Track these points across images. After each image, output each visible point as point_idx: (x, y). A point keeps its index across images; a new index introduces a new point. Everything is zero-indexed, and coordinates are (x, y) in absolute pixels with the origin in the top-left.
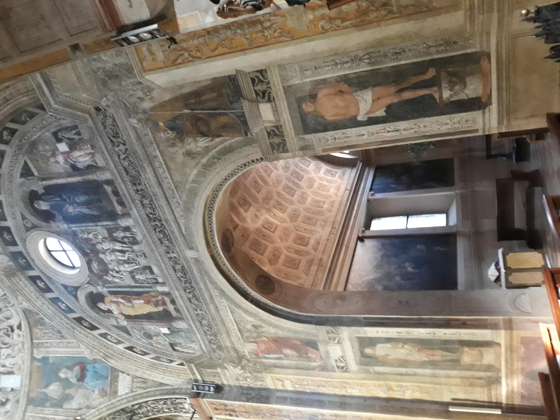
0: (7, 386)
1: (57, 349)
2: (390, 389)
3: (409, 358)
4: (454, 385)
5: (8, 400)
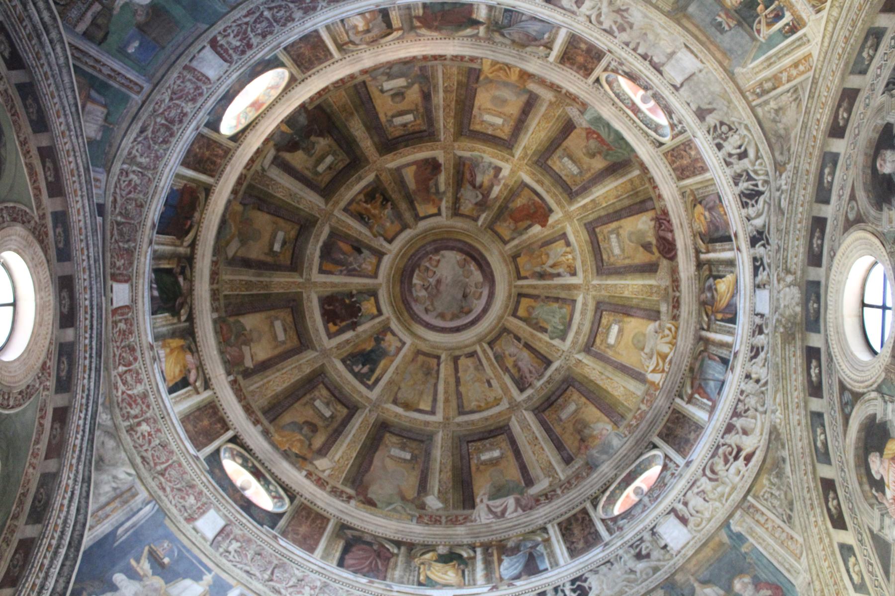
0: (665, 536)
1: (766, 536)
5: (648, 556)
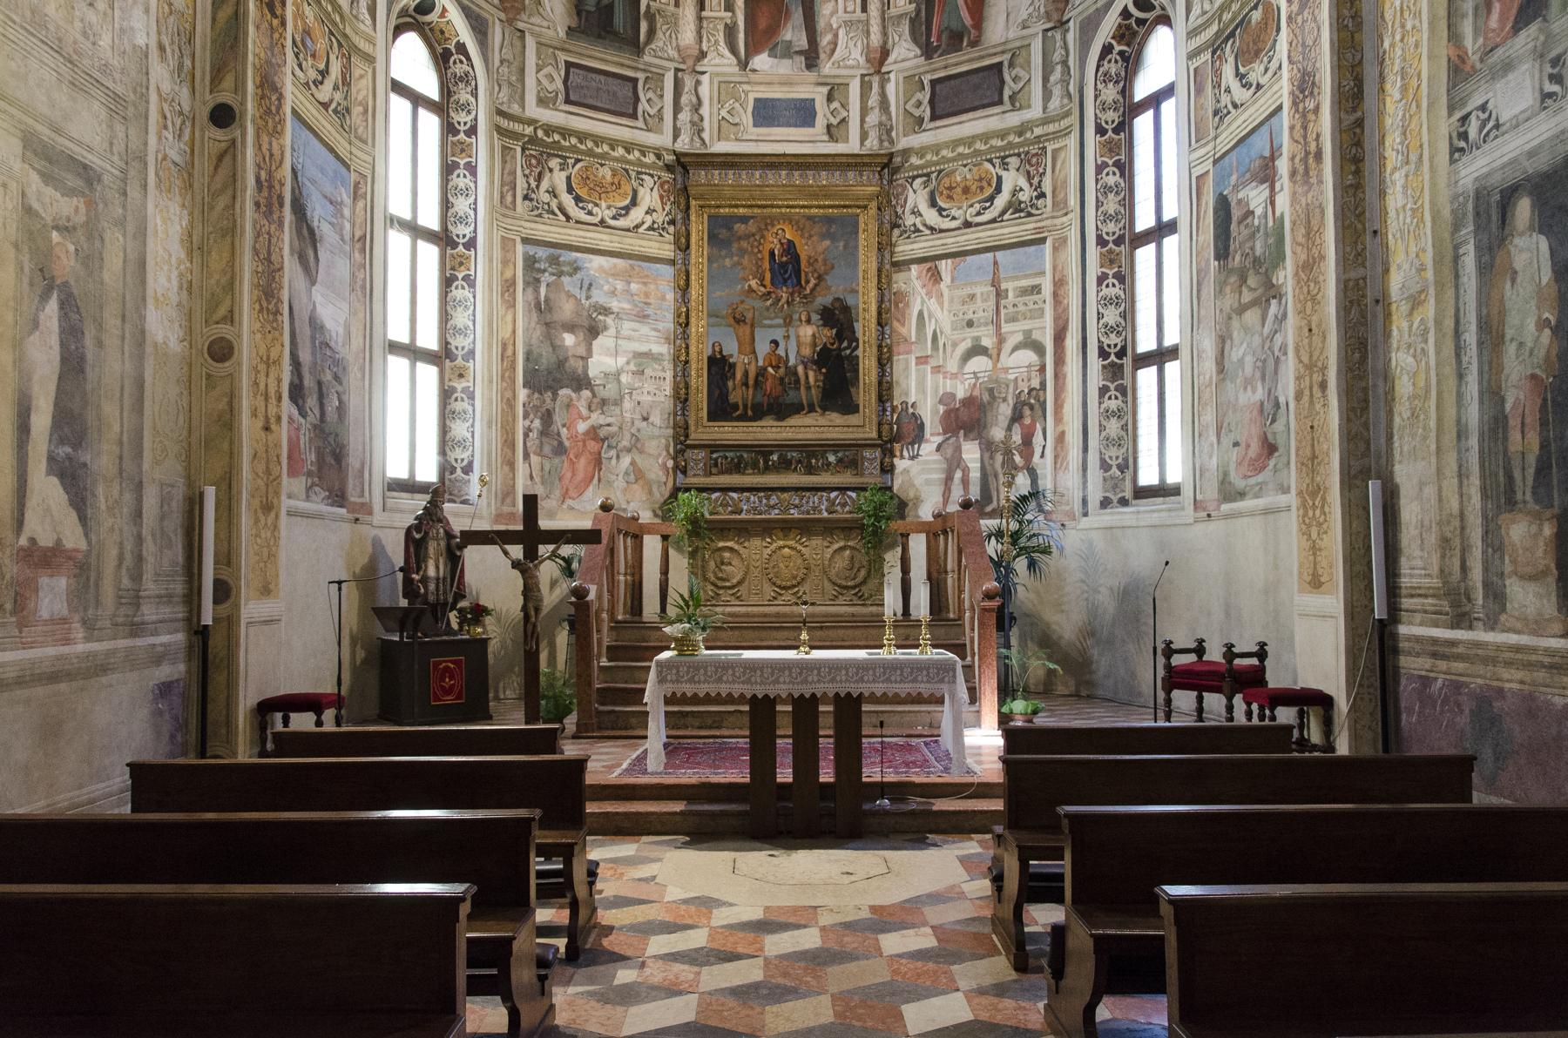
2: (1416, 302)
3: (1511, 349)
4: (1440, 490)
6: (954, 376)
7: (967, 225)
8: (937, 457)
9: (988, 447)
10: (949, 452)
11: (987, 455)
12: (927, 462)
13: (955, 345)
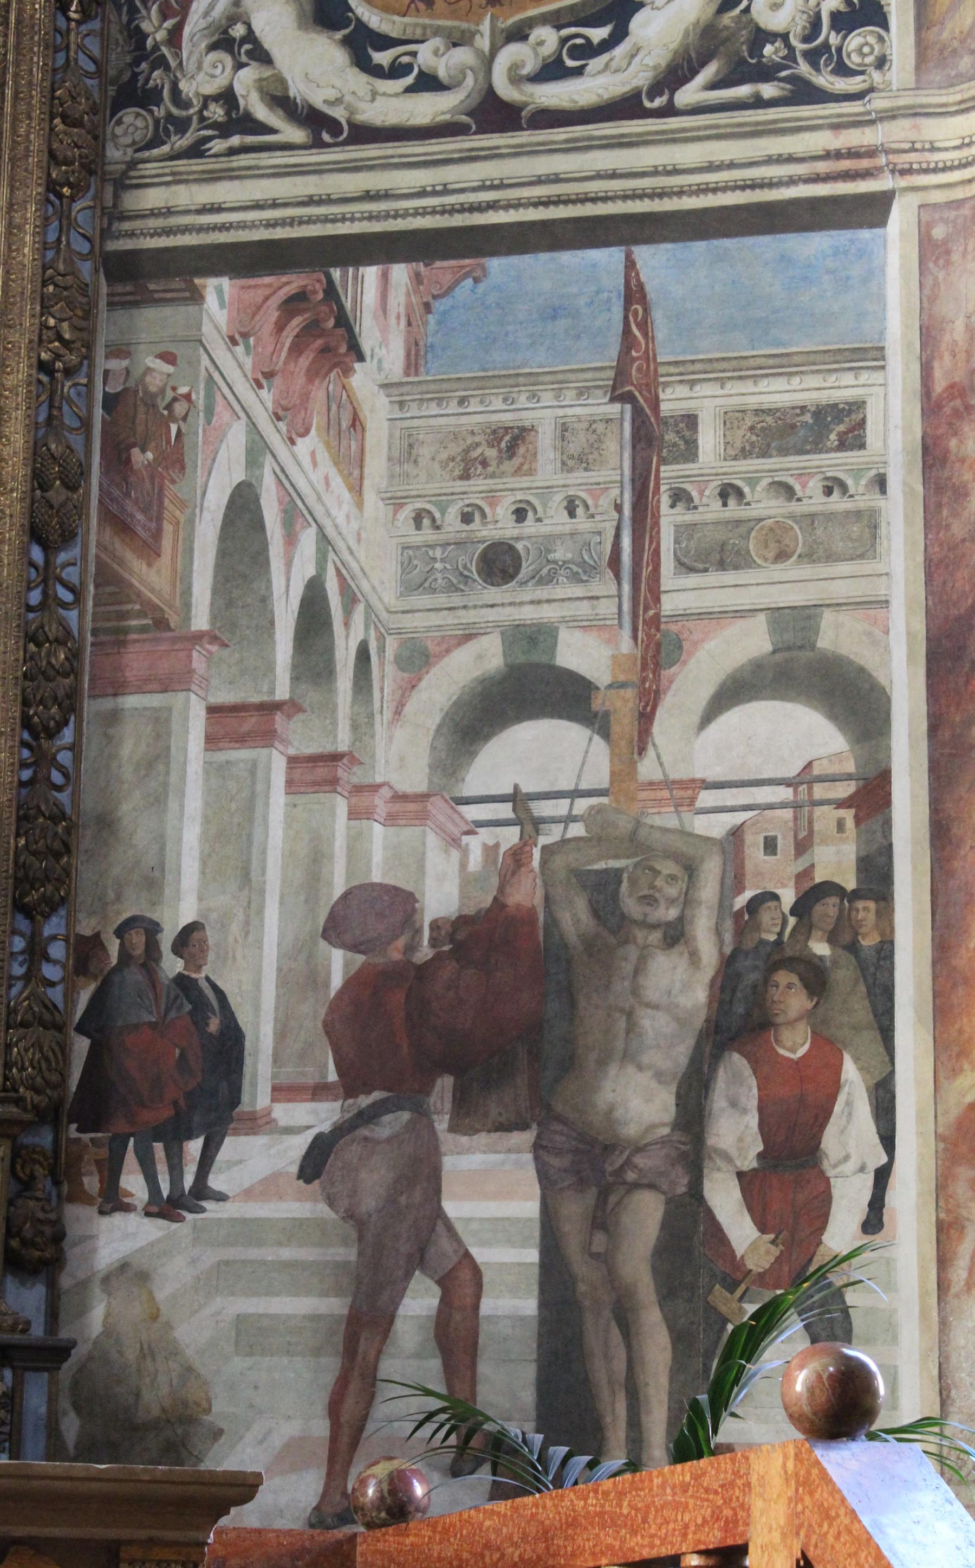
6: (409, 807)
7: (494, 114)
8: (303, 1206)
9: (585, 1168)
10: (373, 1181)
11: (574, 1210)
12: (249, 1231)
13: (417, 659)
